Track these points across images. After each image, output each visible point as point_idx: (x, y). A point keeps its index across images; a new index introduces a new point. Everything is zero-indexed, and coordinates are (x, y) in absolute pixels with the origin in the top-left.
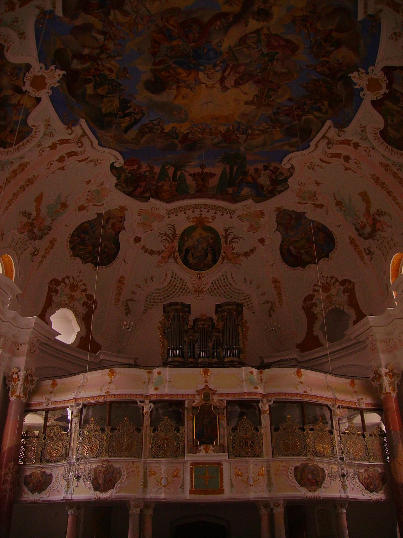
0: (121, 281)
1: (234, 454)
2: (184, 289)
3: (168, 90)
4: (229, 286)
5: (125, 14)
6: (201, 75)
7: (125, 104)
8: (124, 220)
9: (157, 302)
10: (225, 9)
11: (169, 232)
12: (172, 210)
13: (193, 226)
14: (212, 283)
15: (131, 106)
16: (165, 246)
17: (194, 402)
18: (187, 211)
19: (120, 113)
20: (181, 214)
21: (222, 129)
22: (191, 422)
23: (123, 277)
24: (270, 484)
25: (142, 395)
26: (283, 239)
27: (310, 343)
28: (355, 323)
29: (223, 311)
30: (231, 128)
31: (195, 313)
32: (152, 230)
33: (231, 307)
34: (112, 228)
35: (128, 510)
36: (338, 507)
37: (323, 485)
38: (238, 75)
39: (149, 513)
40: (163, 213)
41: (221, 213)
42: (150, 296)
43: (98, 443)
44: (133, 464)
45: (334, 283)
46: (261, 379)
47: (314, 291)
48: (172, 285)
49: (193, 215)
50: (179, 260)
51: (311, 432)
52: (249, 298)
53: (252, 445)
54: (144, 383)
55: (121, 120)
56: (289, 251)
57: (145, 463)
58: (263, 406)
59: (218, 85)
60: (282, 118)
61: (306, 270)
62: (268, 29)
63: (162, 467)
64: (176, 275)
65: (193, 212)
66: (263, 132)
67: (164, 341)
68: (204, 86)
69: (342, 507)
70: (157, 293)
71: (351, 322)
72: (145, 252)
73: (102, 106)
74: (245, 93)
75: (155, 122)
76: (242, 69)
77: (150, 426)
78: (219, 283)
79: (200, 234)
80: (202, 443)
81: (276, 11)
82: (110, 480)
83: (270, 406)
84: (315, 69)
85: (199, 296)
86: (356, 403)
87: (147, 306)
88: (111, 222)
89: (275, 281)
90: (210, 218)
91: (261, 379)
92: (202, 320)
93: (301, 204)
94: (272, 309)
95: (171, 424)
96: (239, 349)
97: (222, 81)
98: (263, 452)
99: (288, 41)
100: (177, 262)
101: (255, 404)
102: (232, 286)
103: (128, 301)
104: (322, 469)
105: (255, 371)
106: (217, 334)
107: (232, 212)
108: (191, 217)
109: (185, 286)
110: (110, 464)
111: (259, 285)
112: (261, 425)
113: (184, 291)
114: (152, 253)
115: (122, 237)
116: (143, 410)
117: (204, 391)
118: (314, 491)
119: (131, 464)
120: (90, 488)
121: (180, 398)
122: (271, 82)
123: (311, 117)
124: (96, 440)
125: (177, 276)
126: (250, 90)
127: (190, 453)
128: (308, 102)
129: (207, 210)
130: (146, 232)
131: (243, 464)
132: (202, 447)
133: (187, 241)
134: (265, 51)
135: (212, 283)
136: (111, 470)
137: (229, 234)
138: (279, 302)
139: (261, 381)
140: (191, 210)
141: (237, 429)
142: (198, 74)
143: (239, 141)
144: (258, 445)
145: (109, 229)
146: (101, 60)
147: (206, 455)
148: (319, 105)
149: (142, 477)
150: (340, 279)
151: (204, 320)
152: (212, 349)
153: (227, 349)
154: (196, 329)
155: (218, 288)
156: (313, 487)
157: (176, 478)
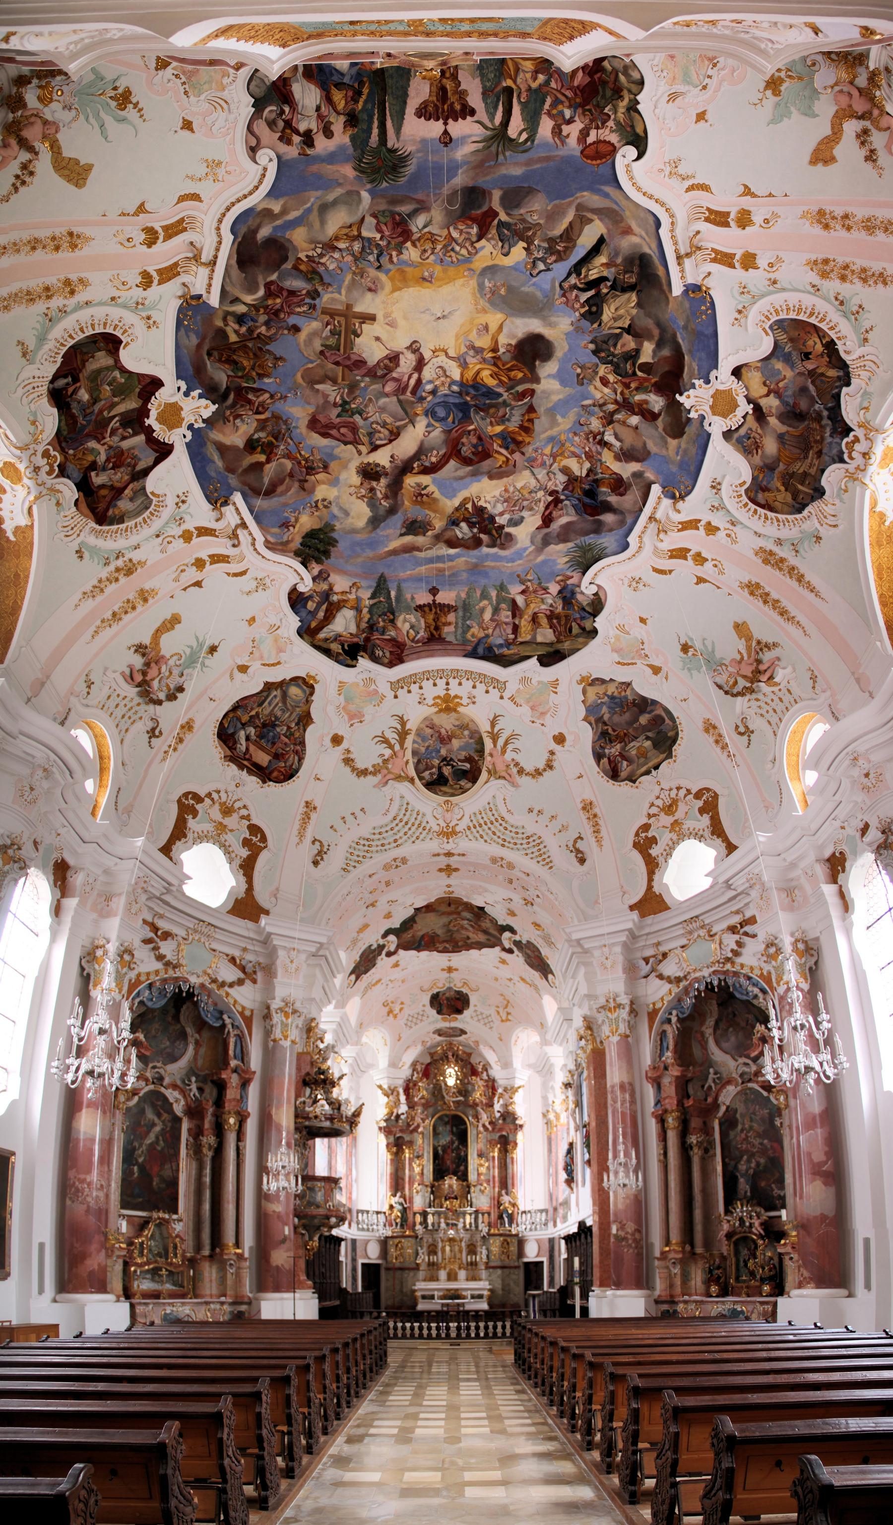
3: (513, 342)
5: (565, 471)
6: (456, 376)
7: (593, 313)
10: (425, 480)
15: (583, 306)
19: (605, 291)
21: (411, 253)
30: (394, 253)
38: (394, 375)
55: (605, 274)
59: (427, 355)
60: (297, 284)
62: (360, 453)
66: (330, 246)
68: (452, 353)
73: (634, 311)
74: (378, 339)
75: (541, 266)
76: (390, 387)
81: (356, 480)
84: (272, 397)
97: (420, 364)
99: (325, 435)
122: (337, 363)
123: (249, 299)
126: (370, 346)
128: (263, 329)
134: (357, 418)
142: (462, 375)
143: (374, 221)
146: (616, 402)
148: (243, 330)
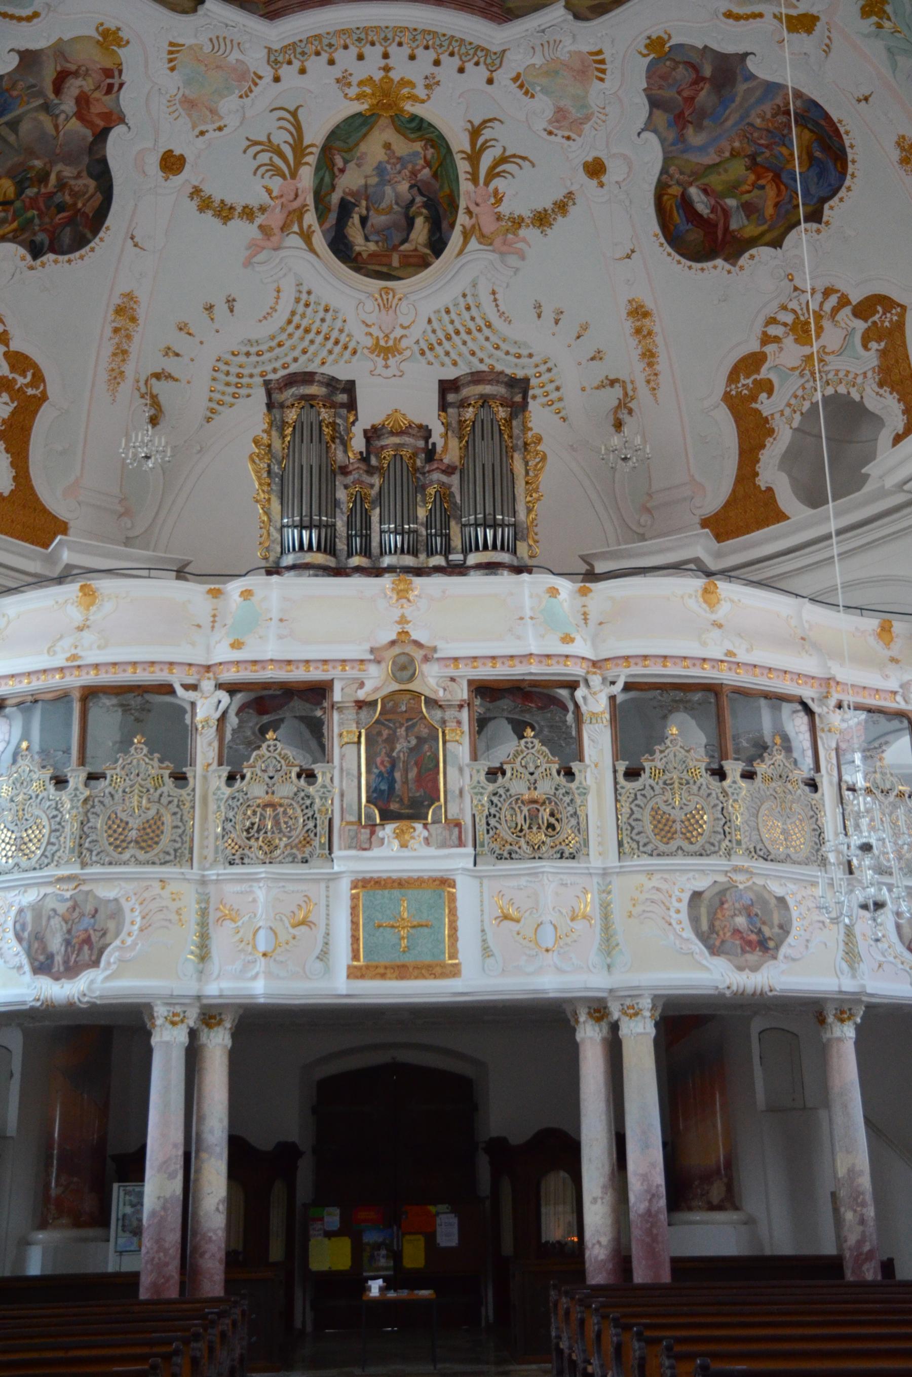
0: (126, 311)
1: (493, 851)
2: (337, 342)
4: (487, 332)
8: (121, 85)
9: (249, 386)
11: (282, 138)
12: (284, 49)
13: (359, 114)
14: (430, 321)
16: (269, 191)
17: (362, 685)
18: (340, 55)
20: (316, 65)
22: (351, 750)
23: (130, 296)
24: (609, 944)
25: (190, 665)
26: (667, 161)
27: (746, 510)
28: (898, 439)
29: (463, 404)
31: (370, 412)
32: (220, 129)
33: (487, 389)
34: (81, 114)
35: (149, 1034)
36: (830, 1019)
37: (784, 950)
39: (217, 1044)
40: (256, 60)
41: (456, 62)
42: (226, 363)
43: (45, 822)
44: (163, 888)
45: (835, 310)
46: (585, 614)
47: (766, 339)
48: (298, 327)
49: (360, 71)
50: (319, 241)
51: (743, 784)
52: (549, 370)
53: (552, 820)
54: (199, 626)
56: (686, 203)
57: (203, 882)
58: (590, 699)
61: (742, 268)
63: (260, 893)
64: (309, 293)
65: (361, 57)
67: (269, 500)
69: (842, 1021)
70: (248, 354)
71: (885, 437)
72: (201, 210)
77: (220, 764)
78: (452, 322)
79: (387, 146)
80: (387, 816)
82: (87, 941)
83: (612, 698)
85: (387, 367)
86: (895, 693)
87: (217, 396)
88: (73, 87)
89: (639, 312)
90: (420, 83)
91: (585, 614)
92: (392, 434)
93: (738, 18)
94: (624, 406)
95: (285, 758)
96: (514, 525)
98: (586, 843)
100: (312, 250)
101: (564, 693)
102: (494, 332)
103: (154, 381)
104: (782, 900)
105: (565, 586)
106: (444, 478)
107: (493, 60)
108: (354, 80)
109: (341, 331)
110: (85, 888)
111: (585, 327)
112: (581, 759)
113: (337, 350)
114: (225, 212)
115: (119, 150)
116: (194, 714)
117: (397, 650)
118: (755, 969)
119: (157, 885)
120: (20, 967)
121: (316, 674)
124: (37, 812)
125: (312, 299)
127: (350, 847)
129: (406, 51)
130: (202, 133)
131: (523, 881)
132: (390, 828)
133: (342, 171)
135: (430, 321)
136: (89, 908)
137: (484, 147)
138: (648, 382)
139: (586, 619)
140: (353, 51)
141: (504, 773)
144: (573, 822)
145: (67, 119)
147: (401, 853)
149: (194, 927)
150: (856, 297)
151: (401, 433)
152: (428, 526)
153: (477, 525)
154: (374, 461)
155: (448, 338)
156: (749, 957)
157: (303, 928)
